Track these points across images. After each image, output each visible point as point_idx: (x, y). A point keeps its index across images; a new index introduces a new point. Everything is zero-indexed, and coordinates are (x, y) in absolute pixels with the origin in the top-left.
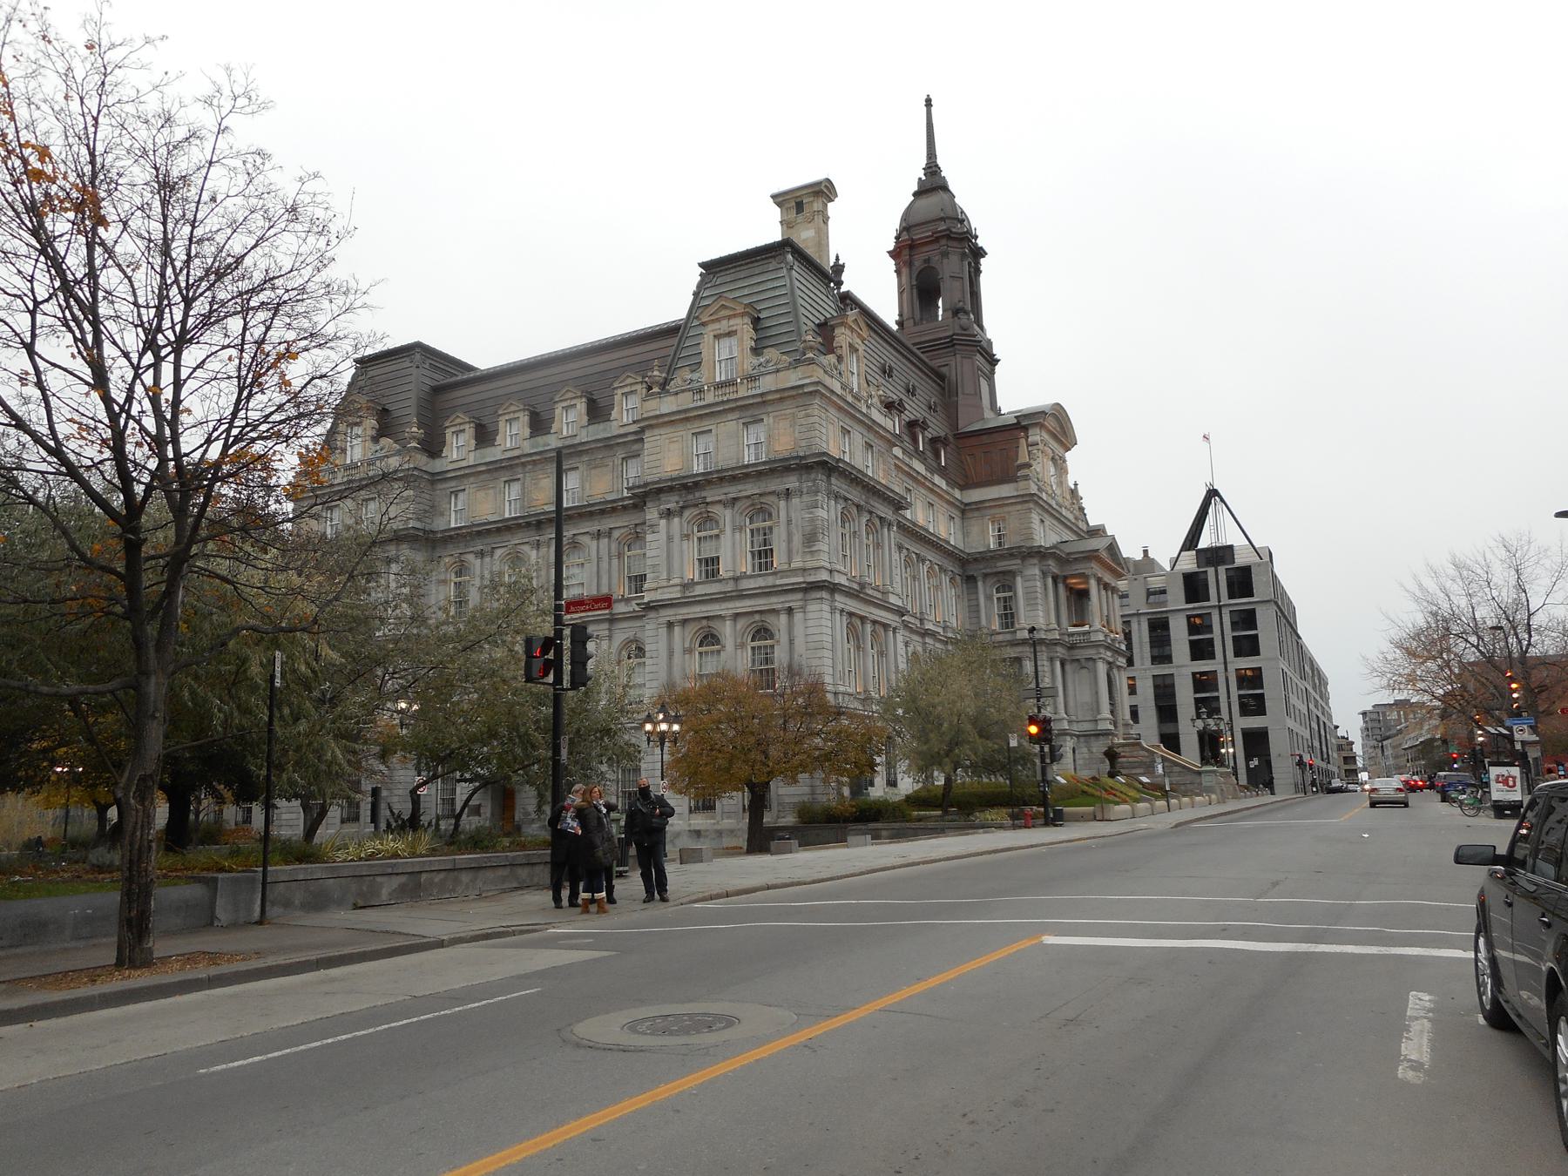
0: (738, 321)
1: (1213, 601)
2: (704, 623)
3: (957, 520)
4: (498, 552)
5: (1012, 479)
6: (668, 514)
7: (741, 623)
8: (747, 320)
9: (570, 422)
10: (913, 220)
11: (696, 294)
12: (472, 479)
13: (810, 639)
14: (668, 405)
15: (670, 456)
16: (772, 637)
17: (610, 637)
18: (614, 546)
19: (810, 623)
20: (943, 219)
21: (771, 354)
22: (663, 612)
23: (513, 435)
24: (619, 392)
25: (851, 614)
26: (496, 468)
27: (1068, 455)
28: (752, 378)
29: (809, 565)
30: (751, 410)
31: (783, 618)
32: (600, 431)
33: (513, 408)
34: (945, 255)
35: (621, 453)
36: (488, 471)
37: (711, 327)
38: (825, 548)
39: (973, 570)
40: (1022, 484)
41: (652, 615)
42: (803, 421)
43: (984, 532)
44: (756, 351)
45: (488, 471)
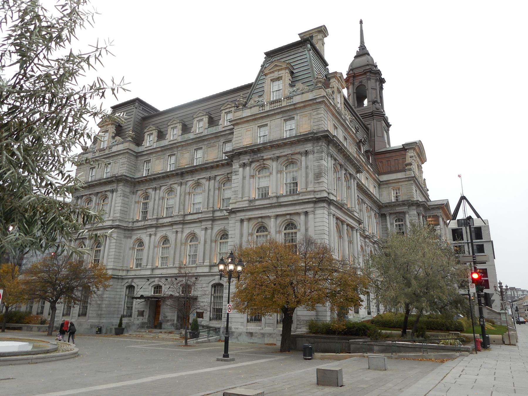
0: (283, 72)
1: (465, 240)
2: (260, 220)
3: (377, 188)
4: (163, 188)
5: (404, 170)
6: (244, 165)
7: (280, 220)
8: (287, 71)
9: (200, 127)
10: (354, 67)
11: (262, 66)
12: (154, 155)
13: (317, 228)
14: (247, 113)
15: (245, 137)
16: (295, 228)
17: (212, 228)
18: (217, 184)
19: (317, 220)
20: (368, 65)
21: (299, 85)
22: (239, 214)
23: (174, 134)
24: (224, 112)
25: (337, 218)
26: (164, 149)
27: (423, 165)
28: (289, 98)
29: (317, 189)
30: (287, 112)
31: (303, 217)
32: (213, 130)
33: (175, 122)
34: (369, 79)
35: (222, 140)
36: (162, 151)
37: (269, 76)
38: (326, 181)
39: (384, 211)
40: (408, 173)
41: (233, 216)
42: (315, 117)
43: (389, 194)
44: (292, 85)
45: (162, 151)
